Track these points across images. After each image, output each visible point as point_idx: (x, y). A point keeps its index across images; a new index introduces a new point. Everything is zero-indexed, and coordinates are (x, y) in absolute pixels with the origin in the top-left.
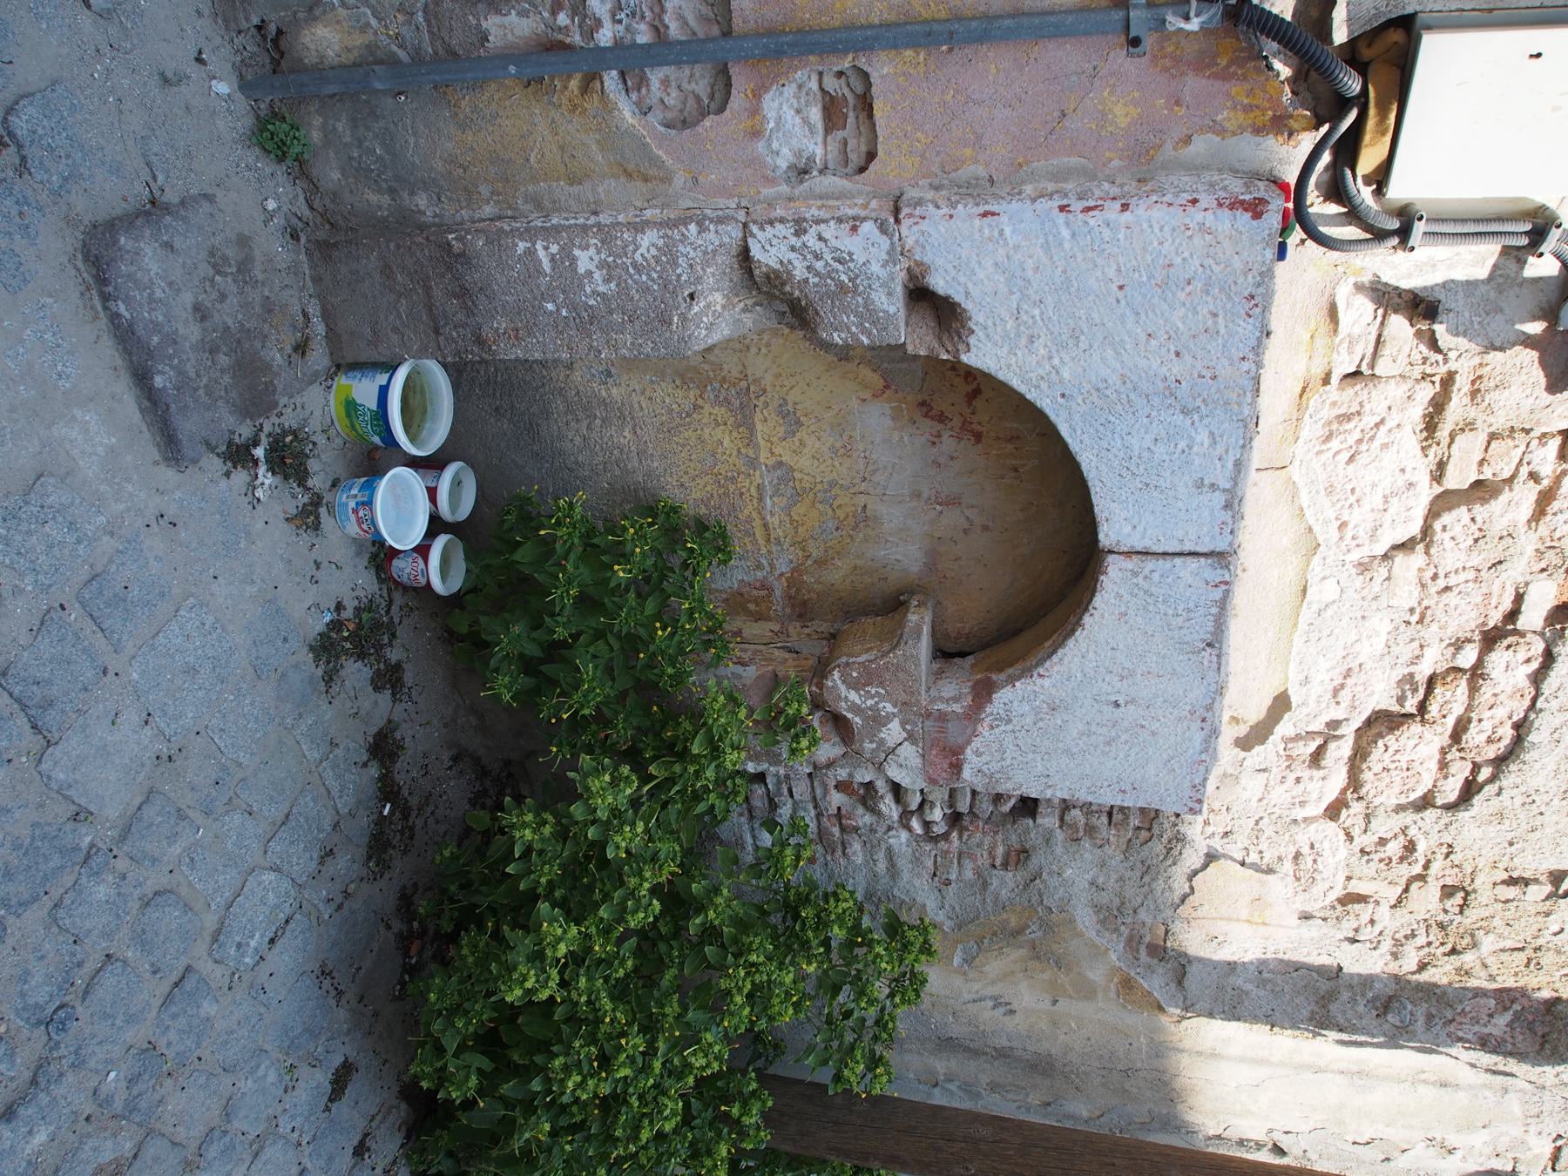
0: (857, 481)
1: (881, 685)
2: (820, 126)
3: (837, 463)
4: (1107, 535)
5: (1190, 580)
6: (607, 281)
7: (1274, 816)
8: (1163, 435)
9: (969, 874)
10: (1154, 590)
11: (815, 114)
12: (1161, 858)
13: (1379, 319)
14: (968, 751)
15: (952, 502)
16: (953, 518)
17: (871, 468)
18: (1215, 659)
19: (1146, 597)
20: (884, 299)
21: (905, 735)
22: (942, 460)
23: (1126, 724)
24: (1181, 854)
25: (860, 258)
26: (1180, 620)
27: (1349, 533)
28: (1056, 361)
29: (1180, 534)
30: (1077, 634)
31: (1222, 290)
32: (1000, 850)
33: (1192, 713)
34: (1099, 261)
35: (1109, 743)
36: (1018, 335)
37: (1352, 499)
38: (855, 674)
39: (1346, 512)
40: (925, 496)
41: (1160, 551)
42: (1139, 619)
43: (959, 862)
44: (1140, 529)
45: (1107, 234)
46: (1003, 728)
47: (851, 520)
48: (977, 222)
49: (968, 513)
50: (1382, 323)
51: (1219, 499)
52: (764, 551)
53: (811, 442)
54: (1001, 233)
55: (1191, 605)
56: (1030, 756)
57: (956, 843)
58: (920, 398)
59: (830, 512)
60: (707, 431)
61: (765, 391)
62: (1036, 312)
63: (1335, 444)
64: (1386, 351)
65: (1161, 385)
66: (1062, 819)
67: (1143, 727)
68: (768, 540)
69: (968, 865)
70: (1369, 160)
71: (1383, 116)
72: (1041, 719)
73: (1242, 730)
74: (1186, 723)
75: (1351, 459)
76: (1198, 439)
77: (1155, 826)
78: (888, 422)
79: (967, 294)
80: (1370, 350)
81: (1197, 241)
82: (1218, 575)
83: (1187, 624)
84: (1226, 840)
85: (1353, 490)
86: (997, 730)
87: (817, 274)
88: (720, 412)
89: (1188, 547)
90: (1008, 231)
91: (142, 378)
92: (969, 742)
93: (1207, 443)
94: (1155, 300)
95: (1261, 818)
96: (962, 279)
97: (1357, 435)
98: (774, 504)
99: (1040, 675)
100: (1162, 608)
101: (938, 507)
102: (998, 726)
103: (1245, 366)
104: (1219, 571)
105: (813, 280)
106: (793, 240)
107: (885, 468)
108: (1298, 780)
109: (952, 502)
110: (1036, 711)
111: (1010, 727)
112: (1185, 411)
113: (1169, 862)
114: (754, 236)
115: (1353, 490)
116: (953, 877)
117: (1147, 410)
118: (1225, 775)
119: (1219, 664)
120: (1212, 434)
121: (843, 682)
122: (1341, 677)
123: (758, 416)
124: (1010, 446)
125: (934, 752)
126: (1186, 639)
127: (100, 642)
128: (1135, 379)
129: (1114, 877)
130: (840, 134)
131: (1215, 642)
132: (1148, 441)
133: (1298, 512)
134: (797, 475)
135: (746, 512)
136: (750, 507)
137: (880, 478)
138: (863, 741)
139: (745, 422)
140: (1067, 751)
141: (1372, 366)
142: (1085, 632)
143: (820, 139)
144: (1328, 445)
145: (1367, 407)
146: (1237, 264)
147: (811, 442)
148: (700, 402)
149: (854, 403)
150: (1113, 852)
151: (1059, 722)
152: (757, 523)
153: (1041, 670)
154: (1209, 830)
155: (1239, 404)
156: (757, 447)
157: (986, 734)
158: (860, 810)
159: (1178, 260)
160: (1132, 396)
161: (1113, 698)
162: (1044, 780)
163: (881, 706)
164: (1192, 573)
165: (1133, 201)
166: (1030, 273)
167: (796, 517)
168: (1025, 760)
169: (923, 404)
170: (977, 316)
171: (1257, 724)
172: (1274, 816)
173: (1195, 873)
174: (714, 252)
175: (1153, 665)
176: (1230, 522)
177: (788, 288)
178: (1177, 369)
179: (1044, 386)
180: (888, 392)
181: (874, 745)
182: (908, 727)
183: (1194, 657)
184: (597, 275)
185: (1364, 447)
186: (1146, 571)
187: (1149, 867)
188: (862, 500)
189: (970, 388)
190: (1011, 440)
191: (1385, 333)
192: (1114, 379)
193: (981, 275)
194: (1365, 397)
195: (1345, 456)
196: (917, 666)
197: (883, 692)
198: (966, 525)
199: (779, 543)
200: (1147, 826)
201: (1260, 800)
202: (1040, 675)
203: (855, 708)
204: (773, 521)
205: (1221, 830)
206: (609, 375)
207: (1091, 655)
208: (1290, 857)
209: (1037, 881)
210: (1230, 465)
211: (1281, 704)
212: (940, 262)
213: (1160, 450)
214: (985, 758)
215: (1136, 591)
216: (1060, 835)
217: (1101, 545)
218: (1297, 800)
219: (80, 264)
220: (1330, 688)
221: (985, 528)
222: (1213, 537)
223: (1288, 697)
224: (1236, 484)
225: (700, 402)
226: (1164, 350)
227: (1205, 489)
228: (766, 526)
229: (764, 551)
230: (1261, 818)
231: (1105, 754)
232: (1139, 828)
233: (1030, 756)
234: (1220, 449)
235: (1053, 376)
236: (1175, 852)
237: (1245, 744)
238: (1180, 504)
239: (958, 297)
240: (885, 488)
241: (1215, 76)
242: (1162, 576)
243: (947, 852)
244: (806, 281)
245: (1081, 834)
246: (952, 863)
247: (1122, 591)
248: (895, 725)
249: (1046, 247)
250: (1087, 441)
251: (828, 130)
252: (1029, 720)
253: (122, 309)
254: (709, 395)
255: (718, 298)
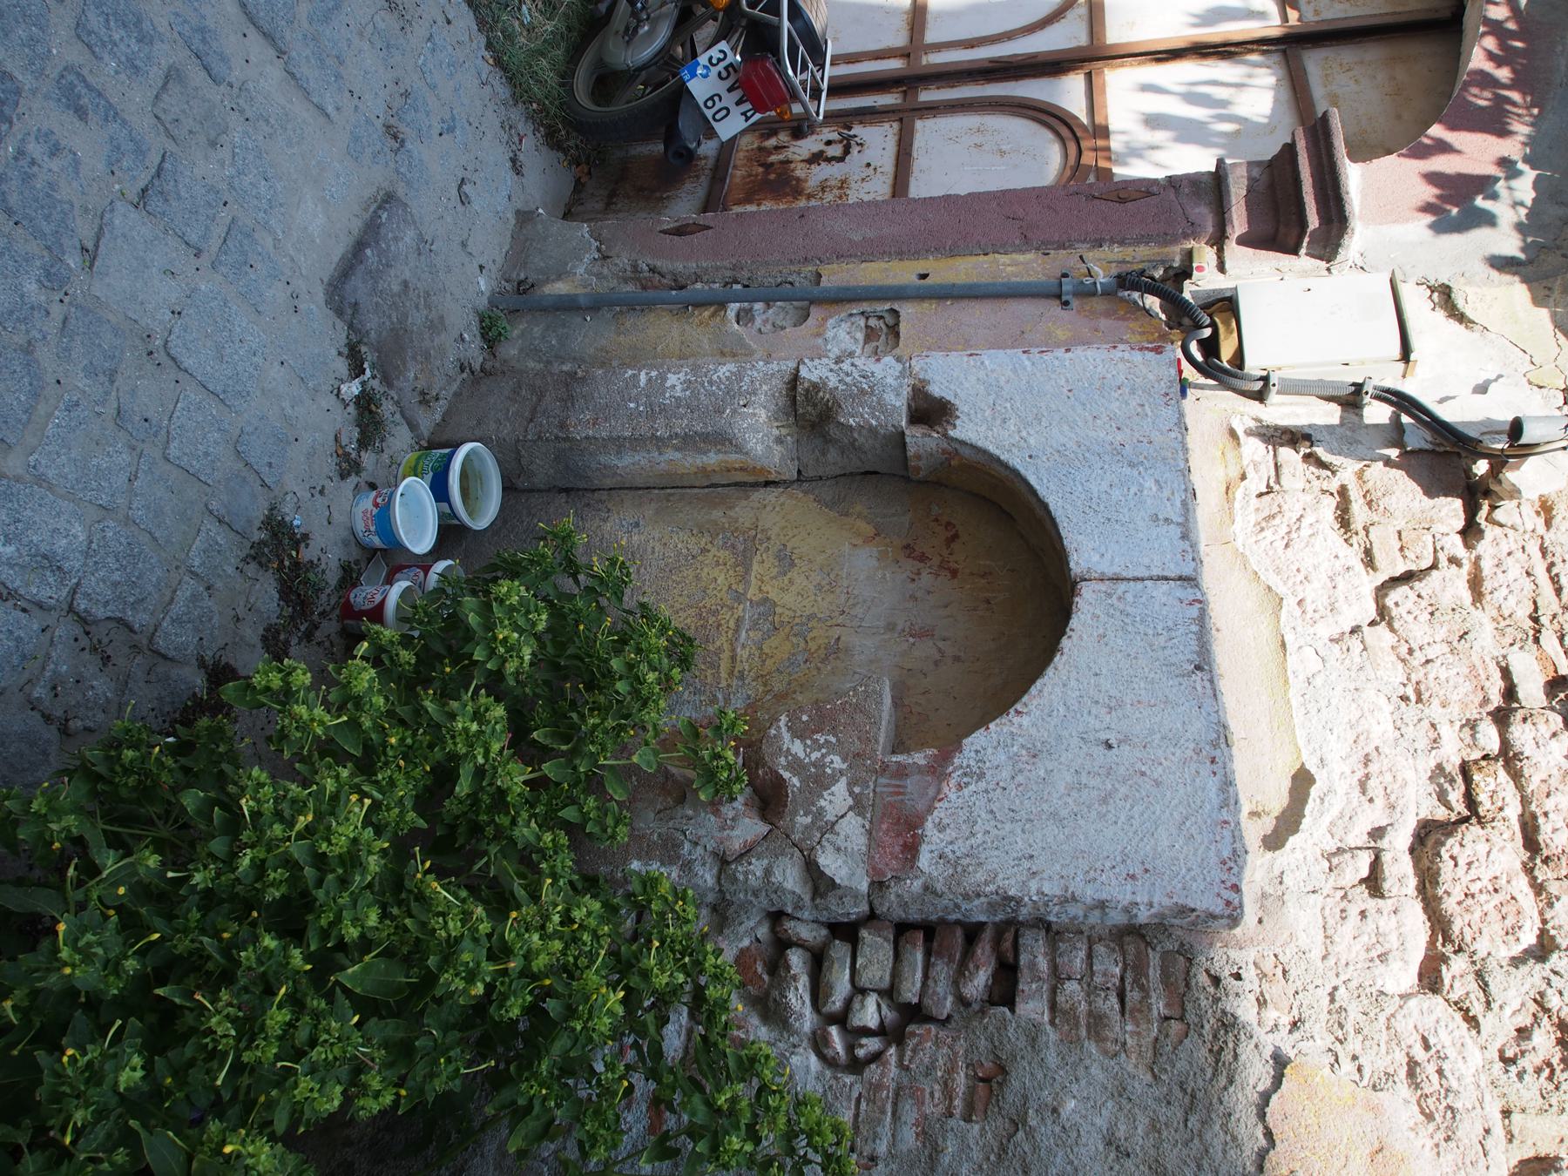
0: (837, 614)
1: (834, 731)
2: (861, 342)
3: (819, 599)
4: (1077, 563)
5: (1164, 599)
6: (684, 390)
7: (1353, 985)
8: (1117, 481)
9: (909, 1137)
10: (1129, 609)
11: (860, 336)
12: (1209, 1072)
13: (1272, 453)
14: (929, 825)
15: (924, 634)
16: (926, 649)
17: (851, 602)
18: (1208, 685)
19: (1123, 617)
20: (893, 397)
21: (850, 801)
22: (918, 594)
23: (1122, 770)
24: (1236, 1056)
25: (879, 375)
26: (1162, 639)
27: (1310, 608)
28: (1024, 434)
29: (1146, 561)
30: (1056, 659)
31: (1144, 391)
32: (961, 1081)
33: (1198, 752)
34: (1053, 376)
35: (1104, 801)
36: (994, 419)
37: (1300, 577)
38: (805, 718)
39: (1299, 588)
40: (900, 627)
41: (1130, 576)
42: (1120, 642)
43: (894, 1113)
44: (1108, 556)
45: (1057, 363)
46: (972, 787)
47: (822, 652)
48: (966, 359)
49: (940, 644)
50: (1275, 455)
51: (1175, 532)
52: (723, 684)
53: (800, 581)
54: (982, 363)
55: (1170, 624)
56: (1008, 826)
57: (893, 1071)
58: (905, 543)
59: (802, 644)
60: (706, 570)
61: (769, 539)
62: (1008, 405)
63: (1268, 533)
64: (1285, 471)
65: (1109, 448)
66: (1053, 1006)
67: (1143, 774)
68: (731, 674)
69: (910, 1113)
70: (1227, 350)
71: (1228, 325)
72: (1021, 771)
73: (1267, 825)
74: (1194, 766)
75: (1287, 546)
76: (1147, 485)
77: (1189, 1006)
78: (874, 563)
79: (956, 395)
80: (1273, 473)
81: (1121, 365)
82: (1190, 594)
83: (1170, 644)
84: (1297, 1035)
85: (1298, 570)
86: (966, 791)
87: (846, 384)
88: (724, 554)
89: (1156, 572)
90: (987, 362)
91: (359, 247)
92: (930, 809)
93: (1154, 489)
94: (1096, 397)
95: (1335, 988)
96: (952, 387)
97: (1285, 529)
98: (748, 637)
99: (1018, 713)
100: (1142, 628)
101: (911, 640)
102: (967, 784)
103: (1173, 435)
104: (1190, 590)
105: (841, 387)
106: (833, 366)
107: (864, 601)
108: (1363, 914)
109: (924, 634)
110: (1014, 759)
111: (982, 785)
112: (1132, 465)
113: (1223, 1081)
114: (804, 363)
115: (1298, 570)
116: (882, 1148)
117: (1100, 464)
118: (1264, 896)
119: (1215, 690)
120: (1157, 481)
121: (789, 729)
122: (1361, 766)
123: (758, 557)
124: (983, 581)
125: (884, 826)
126: (1173, 660)
127: (215, 244)
128: (1088, 444)
129: (1143, 1122)
130: (874, 344)
131: (1203, 664)
132: (1105, 486)
133: (1253, 576)
134: (778, 610)
135: (718, 643)
136: (724, 639)
137: (859, 611)
138: (795, 813)
139: (744, 562)
140: (1054, 815)
141: (1278, 481)
142: (1065, 657)
143: (860, 347)
144: (1263, 534)
145: (1285, 507)
146: (1151, 377)
147: (800, 581)
148: (709, 546)
149: (846, 548)
150: (1133, 1066)
151: (1042, 773)
152: (726, 656)
153: (1018, 706)
154: (1271, 1015)
155: (1175, 459)
156: (748, 584)
157: (952, 796)
158: (755, 1020)
159: (1109, 376)
160: (1087, 455)
161: (1103, 736)
162: (1026, 864)
163: (828, 760)
164: (1164, 594)
165: (1073, 348)
166: (1002, 383)
167: (766, 650)
168: (1001, 833)
169: (907, 547)
170: (963, 407)
171: (1283, 812)
172: (1353, 985)
173: (1266, 1098)
174: (772, 375)
175: (1143, 692)
176: (1190, 550)
177: (821, 394)
178: (1119, 437)
179: (1015, 450)
180: (877, 538)
181: (809, 819)
182: (857, 790)
183: (1185, 681)
184: (678, 388)
185: (1294, 535)
186: (1119, 592)
187: (1193, 1096)
188: (837, 632)
189: (949, 534)
190: (983, 576)
191: (1279, 459)
192: (1071, 445)
193: (967, 385)
194: (1281, 500)
195: (1280, 544)
196: (880, 703)
197: (833, 740)
198: (938, 657)
199: (742, 677)
200: (1176, 1013)
201: (1324, 958)
202: (1018, 713)
203: (796, 765)
204: (742, 654)
205: (1285, 1020)
206: (637, 525)
207: (1073, 683)
208: (1403, 1072)
209: (1021, 1134)
210: (1178, 504)
211: (1302, 781)
212: (937, 378)
213: (1116, 494)
214: (950, 834)
215: (1112, 611)
216: (1052, 1035)
217: (1072, 573)
218: (1374, 954)
219: (381, 193)
220: (1355, 782)
221: (957, 659)
222: (1177, 564)
223: (1308, 772)
224: (1187, 520)
225: (709, 546)
226: (1107, 426)
227: (1161, 523)
228: (733, 658)
229: (723, 684)
230: (1335, 988)
231: (1102, 816)
232: (1167, 1018)
233: (1008, 826)
234: (1166, 493)
235: (1022, 443)
236: (1227, 1056)
237: (1274, 842)
238: (1141, 535)
239: (949, 397)
240: (862, 619)
241: (1119, 319)
242: (1135, 596)
243: (878, 1087)
244: (837, 388)
245: (1083, 1033)
246: (883, 1112)
247: (1098, 612)
248: (840, 788)
249: (1015, 370)
250: (1052, 487)
251: (866, 343)
252: (1005, 774)
253: (385, 216)
254: (719, 541)
255: (763, 415)
